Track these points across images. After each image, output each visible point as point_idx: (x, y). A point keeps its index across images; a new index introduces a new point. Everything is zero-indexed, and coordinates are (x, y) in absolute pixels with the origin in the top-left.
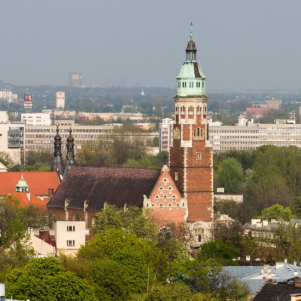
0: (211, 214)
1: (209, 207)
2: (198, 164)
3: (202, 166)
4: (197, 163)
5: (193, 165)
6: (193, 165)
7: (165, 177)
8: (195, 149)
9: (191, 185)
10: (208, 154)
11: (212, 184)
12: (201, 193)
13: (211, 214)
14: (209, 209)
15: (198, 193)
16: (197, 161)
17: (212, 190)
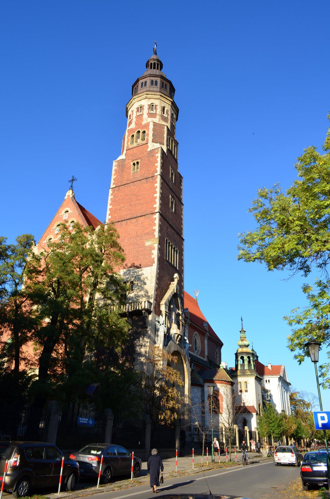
0: (153, 251)
1: (148, 240)
2: (133, 177)
3: (140, 179)
4: (131, 178)
5: (125, 182)
6: (125, 182)
7: (67, 206)
8: (129, 159)
9: (118, 211)
10: (151, 159)
11: (158, 201)
12: (133, 220)
13: (153, 251)
14: (148, 244)
15: (129, 221)
16: (132, 175)
17: (157, 210)
